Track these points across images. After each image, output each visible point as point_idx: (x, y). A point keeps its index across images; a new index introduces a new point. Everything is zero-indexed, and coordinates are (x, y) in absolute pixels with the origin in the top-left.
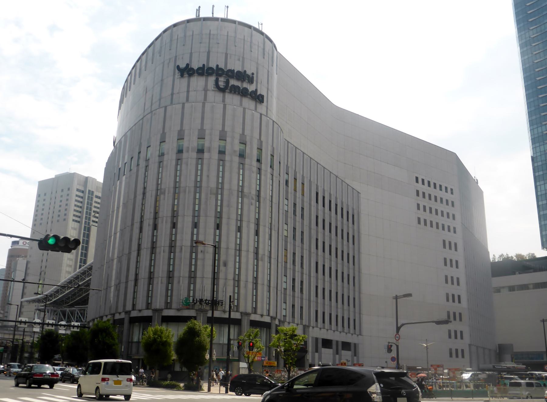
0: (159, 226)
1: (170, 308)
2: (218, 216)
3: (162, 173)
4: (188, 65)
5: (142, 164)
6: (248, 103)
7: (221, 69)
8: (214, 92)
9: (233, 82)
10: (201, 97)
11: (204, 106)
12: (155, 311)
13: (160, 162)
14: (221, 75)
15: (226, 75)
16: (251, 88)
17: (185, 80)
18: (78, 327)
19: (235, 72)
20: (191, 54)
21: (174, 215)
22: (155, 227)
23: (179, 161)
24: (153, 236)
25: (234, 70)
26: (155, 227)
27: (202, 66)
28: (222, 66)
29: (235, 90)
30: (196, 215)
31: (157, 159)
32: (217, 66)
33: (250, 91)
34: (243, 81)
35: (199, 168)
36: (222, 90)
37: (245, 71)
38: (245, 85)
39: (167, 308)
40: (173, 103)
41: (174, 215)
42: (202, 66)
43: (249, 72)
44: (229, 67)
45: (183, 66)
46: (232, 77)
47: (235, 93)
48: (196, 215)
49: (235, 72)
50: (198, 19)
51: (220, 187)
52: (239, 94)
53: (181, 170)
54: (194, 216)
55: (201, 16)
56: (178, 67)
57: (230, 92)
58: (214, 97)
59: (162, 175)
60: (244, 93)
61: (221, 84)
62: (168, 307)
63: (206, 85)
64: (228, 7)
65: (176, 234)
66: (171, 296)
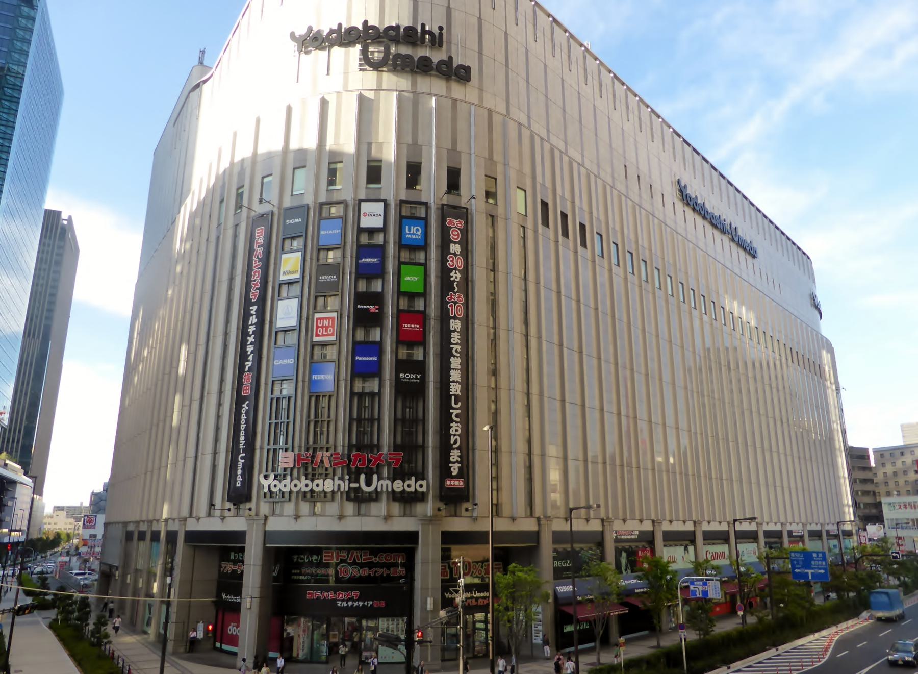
7: (373, 27)
19: (402, 30)
25: (398, 27)
27: (335, 27)
32: (366, 22)
49: (402, 30)
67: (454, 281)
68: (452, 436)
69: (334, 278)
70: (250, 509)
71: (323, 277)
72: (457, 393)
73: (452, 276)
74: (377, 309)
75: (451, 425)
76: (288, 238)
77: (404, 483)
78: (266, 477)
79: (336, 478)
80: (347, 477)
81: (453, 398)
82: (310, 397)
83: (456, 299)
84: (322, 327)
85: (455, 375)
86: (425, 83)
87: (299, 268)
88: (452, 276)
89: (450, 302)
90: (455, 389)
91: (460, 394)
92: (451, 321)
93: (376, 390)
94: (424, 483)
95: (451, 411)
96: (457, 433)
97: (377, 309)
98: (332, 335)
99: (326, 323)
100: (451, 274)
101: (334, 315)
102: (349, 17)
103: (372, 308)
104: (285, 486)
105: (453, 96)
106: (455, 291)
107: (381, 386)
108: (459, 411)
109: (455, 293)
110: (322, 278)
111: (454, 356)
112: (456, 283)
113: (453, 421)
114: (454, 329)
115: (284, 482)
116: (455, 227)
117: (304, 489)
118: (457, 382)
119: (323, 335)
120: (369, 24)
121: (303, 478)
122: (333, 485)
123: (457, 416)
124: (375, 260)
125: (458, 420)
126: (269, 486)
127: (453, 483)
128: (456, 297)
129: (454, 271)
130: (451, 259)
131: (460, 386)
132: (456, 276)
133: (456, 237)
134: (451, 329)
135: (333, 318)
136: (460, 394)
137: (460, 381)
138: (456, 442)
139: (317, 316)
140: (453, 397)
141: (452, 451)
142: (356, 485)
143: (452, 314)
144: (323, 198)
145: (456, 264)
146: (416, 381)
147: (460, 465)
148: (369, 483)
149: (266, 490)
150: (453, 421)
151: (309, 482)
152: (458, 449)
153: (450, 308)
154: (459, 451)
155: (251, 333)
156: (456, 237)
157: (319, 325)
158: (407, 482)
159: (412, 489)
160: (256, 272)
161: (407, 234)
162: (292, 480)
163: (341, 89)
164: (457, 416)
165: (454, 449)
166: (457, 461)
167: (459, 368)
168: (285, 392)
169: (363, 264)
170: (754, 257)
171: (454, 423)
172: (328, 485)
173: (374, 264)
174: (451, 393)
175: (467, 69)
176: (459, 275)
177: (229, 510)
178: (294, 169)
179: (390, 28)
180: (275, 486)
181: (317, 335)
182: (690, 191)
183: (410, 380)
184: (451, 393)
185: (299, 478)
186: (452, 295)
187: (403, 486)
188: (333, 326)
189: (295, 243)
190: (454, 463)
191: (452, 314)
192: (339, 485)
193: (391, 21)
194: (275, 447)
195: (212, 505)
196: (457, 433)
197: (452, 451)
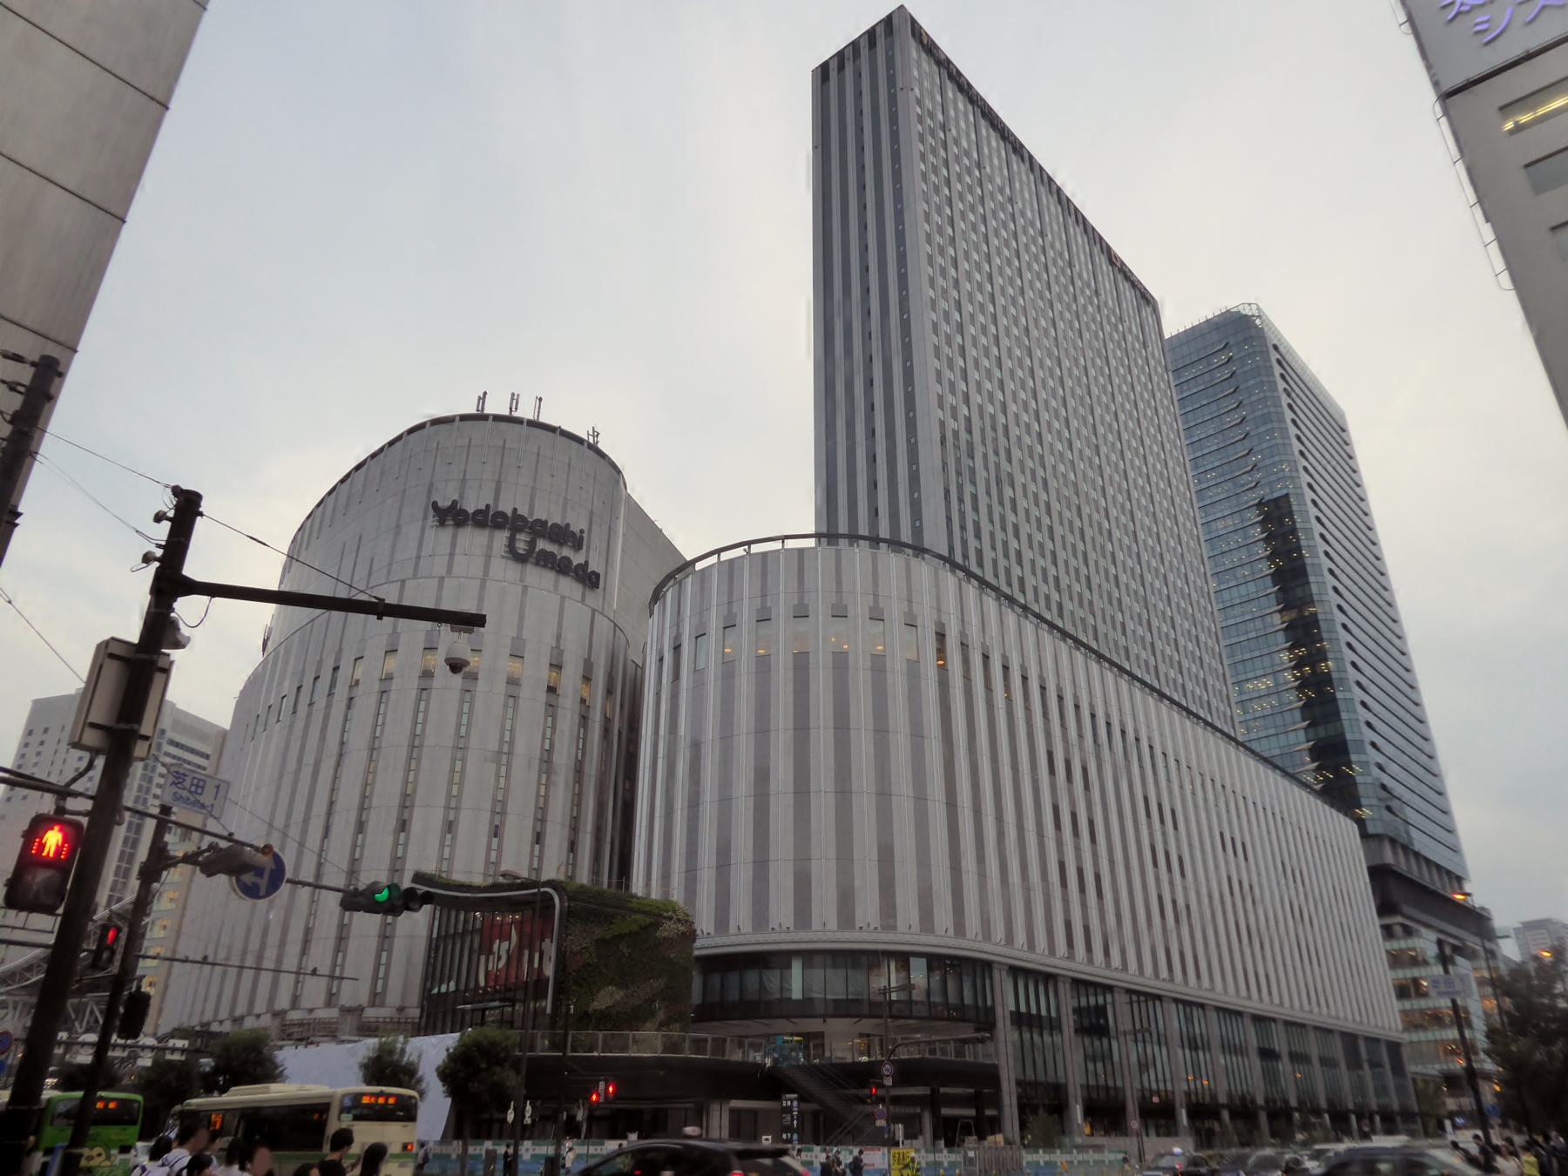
0: (371, 827)
1: (382, 1005)
2: (498, 810)
3: (385, 714)
4: (455, 503)
5: (341, 692)
6: (569, 586)
7: (523, 518)
8: (504, 560)
9: (542, 545)
10: (477, 570)
11: (483, 587)
12: (346, 1011)
13: (383, 692)
14: (520, 530)
15: (530, 528)
16: (577, 559)
17: (446, 534)
18: (183, 1051)
19: (549, 524)
20: (464, 480)
21: (406, 802)
22: (361, 827)
23: (424, 692)
24: (354, 846)
25: (546, 522)
26: (361, 827)
27: (483, 507)
28: (523, 511)
29: (546, 561)
30: (453, 805)
31: (376, 686)
32: (515, 510)
33: (575, 563)
34: (562, 544)
35: (466, 710)
36: (521, 559)
37: (568, 525)
38: (566, 552)
39: (372, 1004)
40: (419, 575)
41: (406, 802)
42: (483, 507)
43: (575, 528)
44: (540, 514)
45: (444, 503)
46: (542, 536)
47: (545, 566)
48: (453, 805)
49: (549, 524)
50: (481, 417)
51: (506, 749)
52: (552, 568)
53: (426, 711)
54: (447, 808)
55: (486, 412)
56: (435, 505)
57: (537, 564)
58: (505, 571)
59: (384, 718)
60: (562, 567)
61: (521, 546)
62: (377, 1002)
63: (490, 547)
64: (540, 399)
65: (406, 844)
66: (386, 978)
120: (519, 512)
175: (597, 576)
179: (538, 521)
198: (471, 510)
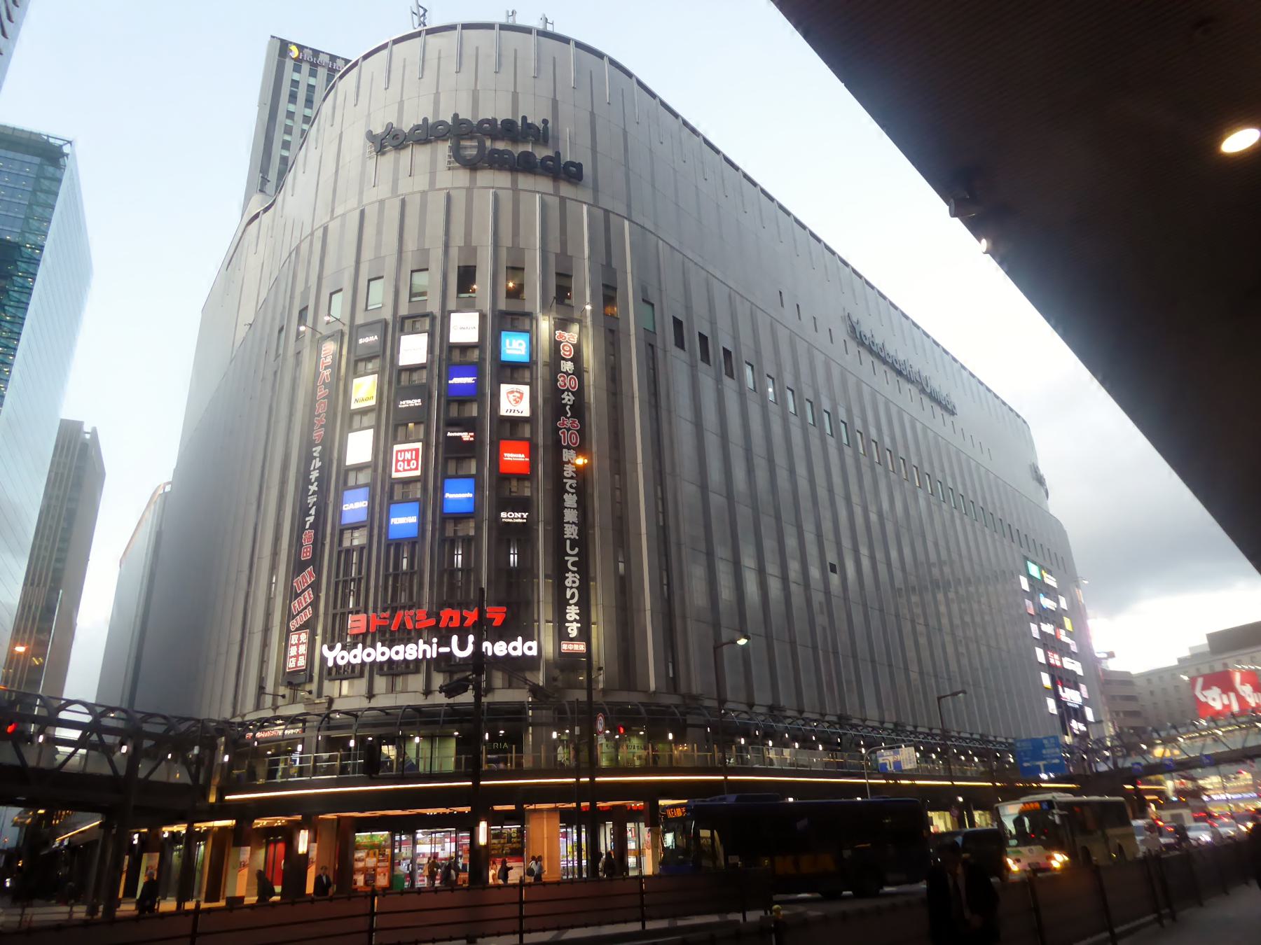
7: (466, 121)
16: (541, 153)
19: (499, 122)
32: (456, 116)
49: (499, 122)
67: (566, 405)
68: (568, 589)
69: (417, 402)
70: (310, 692)
71: (404, 402)
72: (572, 537)
73: (564, 399)
74: (471, 436)
75: (567, 575)
76: (361, 360)
77: (508, 645)
78: (331, 648)
79: (421, 641)
80: (435, 640)
81: (568, 542)
82: (388, 546)
83: (569, 425)
84: (403, 461)
85: (570, 515)
86: (525, 181)
87: (374, 394)
88: (564, 399)
89: (562, 429)
90: (571, 532)
91: (577, 538)
92: (564, 450)
93: (472, 533)
94: (534, 644)
95: (566, 558)
96: (574, 585)
97: (471, 436)
98: (416, 469)
99: (408, 456)
100: (563, 396)
101: (419, 445)
102: (436, 111)
103: (466, 436)
104: (355, 657)
105: (562, 194)
106: (568, 416)
107: (478, 528)
108: (577, 559)
109: (568, 418)
110: (404, 404)
111: (568, 493)
112: (568, 407)
113: (569, 571)
114: (567, 460)
115: (354, 652)
116: (567, 342)
117: (380, 659)
118: (573, 523)
119: (405, 470)
121: (379, 644)
122: (417, 651)
123: (573, 564)
124: (470, 380)
125: (575, 569)
126: (335, 658)
127: (571, 647)
128: (567, 422)
129: (566, 393)
130: (562, 378)
131: (576, 528)
132: (568, 398)
133: (568, 353)
134: (564, 460)
135: (417, 450)
136: (577, 538)
137: (577, 522)
138: (573, 596)
139: (397, 447)
140: (568, 542)
141: (568, 607)
142: (446, 650)
143: (565, 443)
144: (404, 310)
145: (568, 384)
146: (521, 521)
147: (579, 625)
148: (462, 646)
149: (330, 664)
150: (569, 571)
151: (385, 649)
152: (575, 604)
153: (562, 436)
154: (577, 608)
155: (313, 480)
156: (568, 353)
157: (399, 458)
158: (513, 644)
159: (519, 653)
160: (322, 403)
161: (509, 349)
162: (364, 648)
163: (427, 188)
164: (573, 564)
165: (570, 605)
166: (575, 620)
167: (575, 506)
168: (356, 542)
169: (454, 385)
170: (953, 413)
171: (570, 573)
172: (410, 652)
173: (467, 385)
174: (565, 536)
176: (572, 398)
177: (283, 696)
178: (369, 281)
180: (343, 658)
181: (397, 471)
182: (865, 328)
183: (515, 521)
184: (565, 536)
185: (374, 646)
186: (564, 421)
187: (507, 649)
188: (417, 459)
189: (370, 366)
190: (572, 622)
191: (565, 443)
192: (425, 652)
193: (486, 113)
194: (343, 610)
195: (261, 689)
196: (574, 585)
197: (568, 607)
198: (406, 130)
